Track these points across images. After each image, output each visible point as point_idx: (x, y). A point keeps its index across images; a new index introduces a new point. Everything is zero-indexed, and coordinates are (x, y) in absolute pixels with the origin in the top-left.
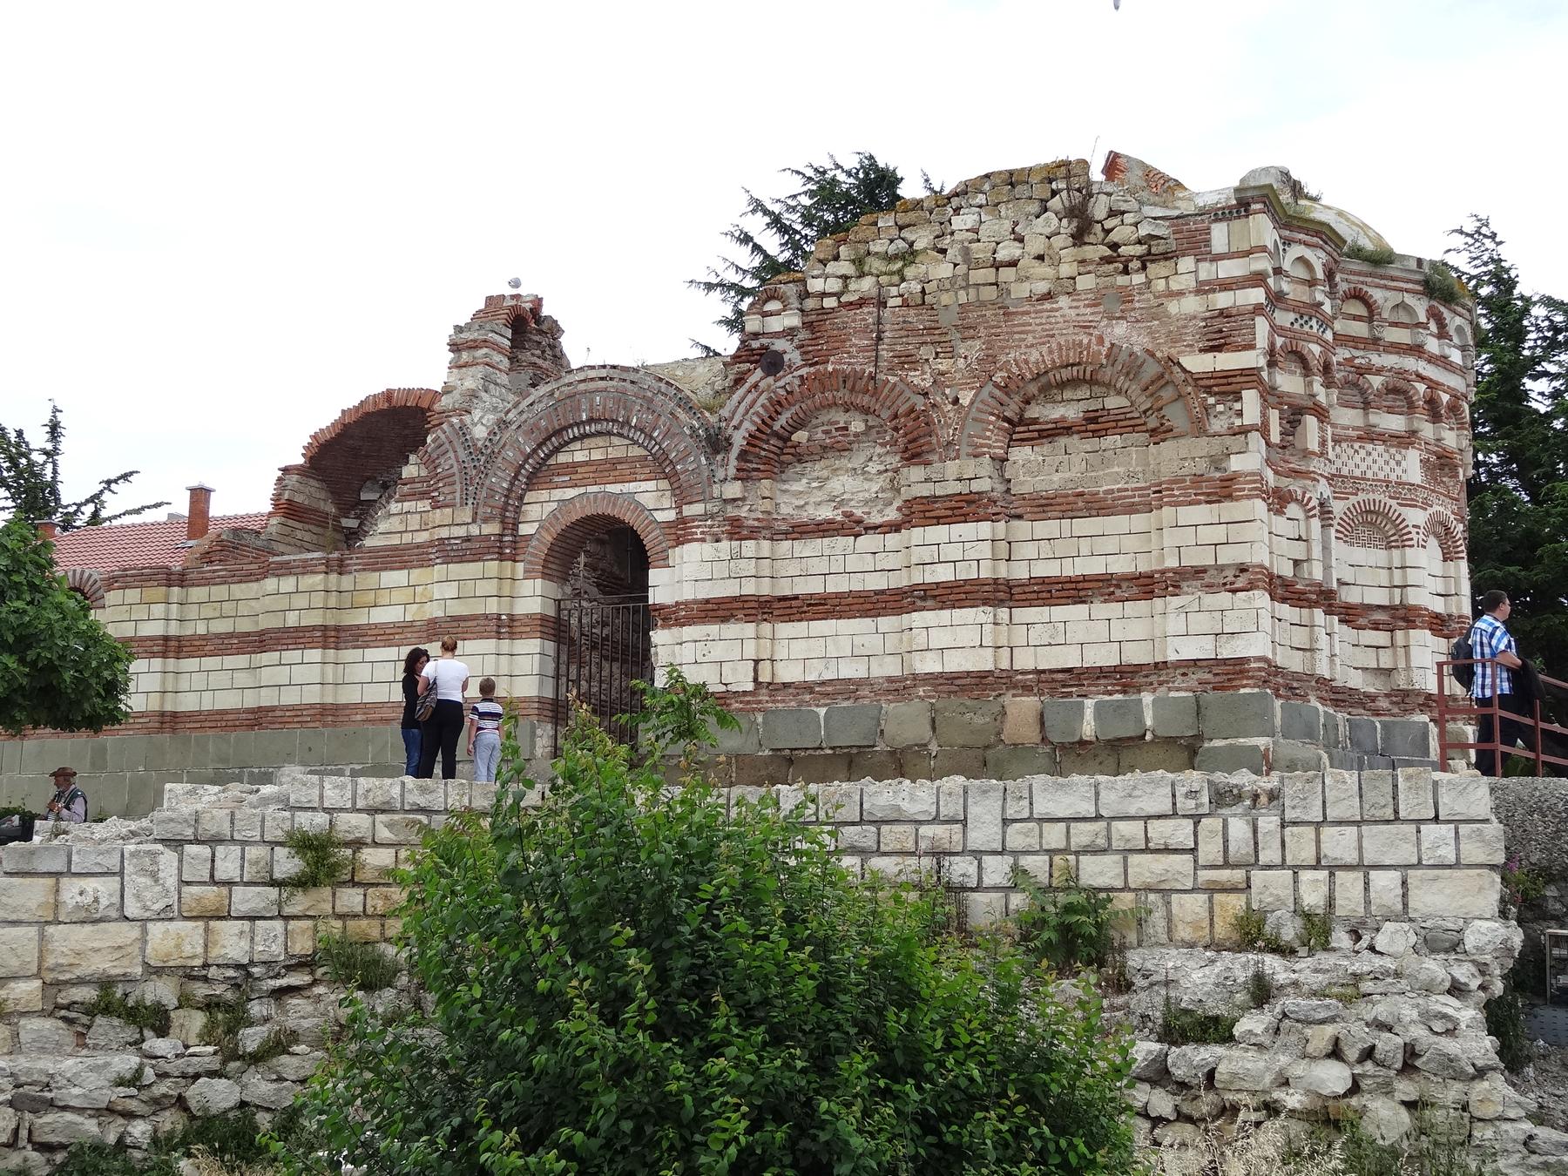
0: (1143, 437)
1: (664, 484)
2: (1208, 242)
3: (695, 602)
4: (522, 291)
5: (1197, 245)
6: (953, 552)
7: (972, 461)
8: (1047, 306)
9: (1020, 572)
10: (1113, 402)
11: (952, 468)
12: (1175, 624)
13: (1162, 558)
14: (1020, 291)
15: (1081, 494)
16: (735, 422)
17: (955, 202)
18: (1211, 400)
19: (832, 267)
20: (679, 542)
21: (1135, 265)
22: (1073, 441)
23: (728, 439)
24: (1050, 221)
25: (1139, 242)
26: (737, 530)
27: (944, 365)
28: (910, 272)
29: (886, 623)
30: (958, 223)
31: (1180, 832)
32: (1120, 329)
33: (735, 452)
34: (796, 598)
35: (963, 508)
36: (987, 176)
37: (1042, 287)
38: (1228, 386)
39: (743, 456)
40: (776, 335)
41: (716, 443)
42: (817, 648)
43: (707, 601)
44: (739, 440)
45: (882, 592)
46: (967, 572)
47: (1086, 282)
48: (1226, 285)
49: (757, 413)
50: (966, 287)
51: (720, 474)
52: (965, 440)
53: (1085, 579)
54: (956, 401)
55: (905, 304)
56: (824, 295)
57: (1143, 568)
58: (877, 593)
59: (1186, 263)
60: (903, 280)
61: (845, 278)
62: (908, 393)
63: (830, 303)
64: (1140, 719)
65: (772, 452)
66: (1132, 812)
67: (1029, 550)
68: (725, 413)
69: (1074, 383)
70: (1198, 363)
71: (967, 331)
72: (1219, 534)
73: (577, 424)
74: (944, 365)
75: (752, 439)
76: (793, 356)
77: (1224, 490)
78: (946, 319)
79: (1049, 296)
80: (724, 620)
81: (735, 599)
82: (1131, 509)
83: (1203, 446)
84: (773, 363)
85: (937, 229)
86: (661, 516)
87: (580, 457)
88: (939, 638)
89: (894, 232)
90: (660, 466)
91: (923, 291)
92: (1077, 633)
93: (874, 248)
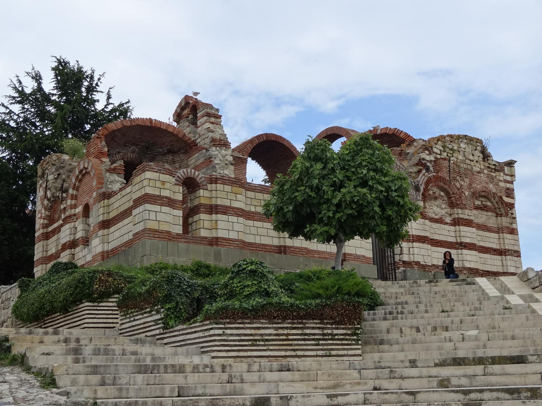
2: (504, 170)
3: (416, 235)
4: (199, 97)
5: (502, 170)
10: (489, 204)
11: (466, 211)
13: (504, 246)
19: (437, 146)
28: (454, 155)
32: (491, 186)
33: (421, 193)
35: (468, 223)
36: (466, 136)
37: (478, 170)
40: (427, 161)
41: (417, 189)
50: (465, 164)
51: (419, 198)
56: (437, 154)
57: (498, 248)
58: (451, 242)
59: (502, 174)
61: (440, 150)
63: (438, 156)
68: (418, 179)
70: (506, 199)
72: (513, 242)
74: (462, 183)
76: (431, 169)
78: (462, 170)
79: (479, 172)
80: (423, 242)
84: (428, 169)
88: (469, 258)
92: (489, 262)
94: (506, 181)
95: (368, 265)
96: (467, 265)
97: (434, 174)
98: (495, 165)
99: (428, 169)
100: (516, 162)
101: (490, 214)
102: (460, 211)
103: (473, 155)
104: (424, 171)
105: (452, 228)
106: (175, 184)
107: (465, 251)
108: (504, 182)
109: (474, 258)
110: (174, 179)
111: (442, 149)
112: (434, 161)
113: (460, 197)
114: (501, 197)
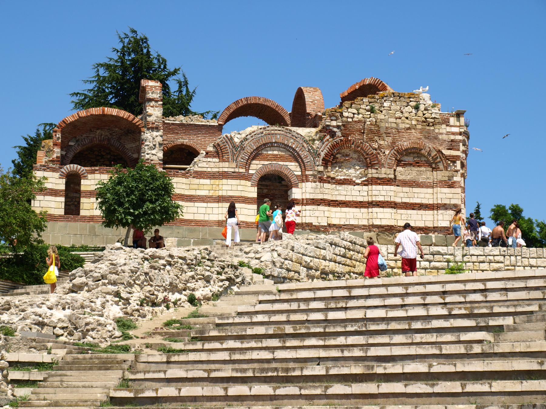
0: (431, 169)
1: (297, 164)
6: (383, 193)
7: (389, 170)
8: (409, 131)
9: (398, 200)
12: (440, 217)
14: (402, 126)
15: (414, 182)
16: (321, 149)
17: (385, 98)
18: (449, 162)
19: (350, 110)
20: (303, 181)
21: (431, 124)
22: (413, 168)
23: (319, 154)
24: (409, 109)
25: (431, 118)
26: (321, 180)
27: (382, 142)
29: (363, 210)
30: (386, 104)
31: (501, 258)
33: (322, 158)
34: (337, 201)
37: (408, 126)
38: (454, 159)
39: (324, 159)
40: (334, 127)
42: (343, 215)
43: (313, 199)
44: (323, 155)
45: (362, 202)
46: (388, 199)
47: (419, 127)
48: (453, 134)
49: (328, 148)
52: (387, 164)
53: (416, 204)
54: (384, 153)
55: (371, 124)
56: (347, 117)
58: (360, 202)
59: (444, 126)
60: (370, 117)
61: (354, 114)
62: (371, 149)
63: (350, 120)
64: (432, 240)
65: (330, 160)
66: (491, 254)
67: (402, 195)
69: (414, 153)
70: (446, 152)
71: (388, 134)
72: (451, 196)
73: (271, 143)
74: (382, 142)
75: (326, 155)
76: (339, 134)
77: (451, 185)
78: (382, 131)
79: (409, 129)
80: (319, 205)
81: (321, 199)
82: (428, 187)
83: (447, 173)
84: (333, 135)
85: (380, 105)
86: (296, 173)
87: (270, 153)
88: (380, 215)
89: (368, 103)
90: (296, 158)
91: (376, 122)
93: (362, 106)
94: (448, 133)
95: (250, 229)
96: (377, 222)
97: (342, 138)
98: (435, 118)
99: (333, 135)
100: (465, 111)
101: (423, 169)
102: (374, 171)
103: (402, 112)
104: (328, 137)
105: (365, 188)
106: (60, 178)
107: (375, 210)
108: (446, 134)
109: (388, 216)
110: (59, 173)
111: (355, 111)
112: (344, 125)
113: (377, 157)
114: (440, 152)
